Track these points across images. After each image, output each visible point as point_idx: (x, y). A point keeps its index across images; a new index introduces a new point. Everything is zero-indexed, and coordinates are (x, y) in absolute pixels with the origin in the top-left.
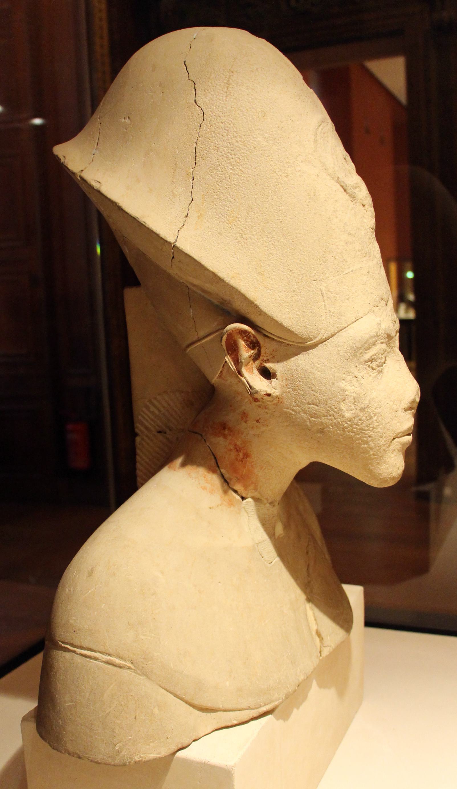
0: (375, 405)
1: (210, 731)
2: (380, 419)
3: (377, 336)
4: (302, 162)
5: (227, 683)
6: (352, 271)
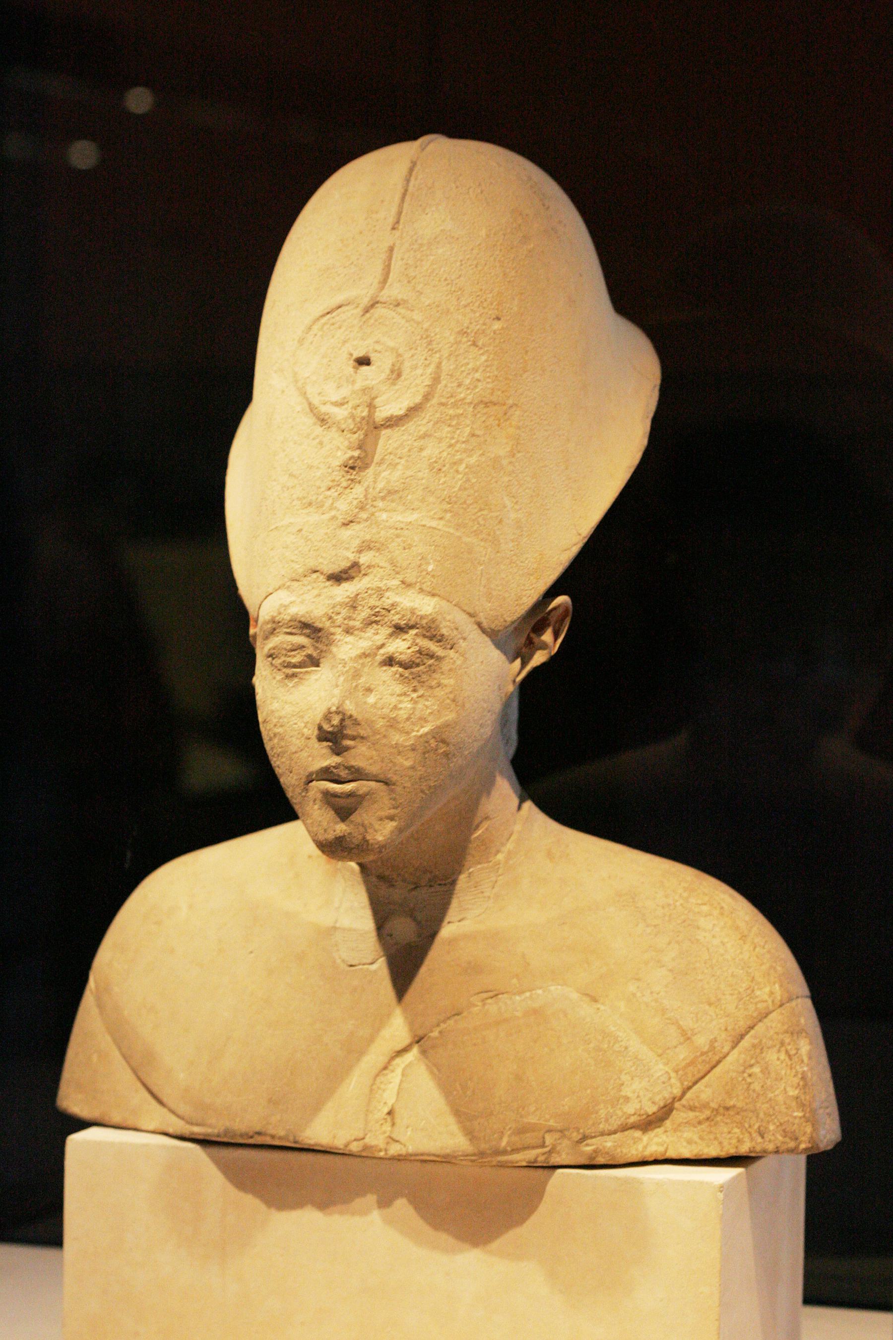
0: (275, 721)
1: (151, 1128)
2: (283, 744)
3: (274, 622)
4: (276, 372)
5: (182, 1076)
6: (276, 528)
